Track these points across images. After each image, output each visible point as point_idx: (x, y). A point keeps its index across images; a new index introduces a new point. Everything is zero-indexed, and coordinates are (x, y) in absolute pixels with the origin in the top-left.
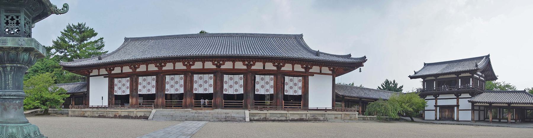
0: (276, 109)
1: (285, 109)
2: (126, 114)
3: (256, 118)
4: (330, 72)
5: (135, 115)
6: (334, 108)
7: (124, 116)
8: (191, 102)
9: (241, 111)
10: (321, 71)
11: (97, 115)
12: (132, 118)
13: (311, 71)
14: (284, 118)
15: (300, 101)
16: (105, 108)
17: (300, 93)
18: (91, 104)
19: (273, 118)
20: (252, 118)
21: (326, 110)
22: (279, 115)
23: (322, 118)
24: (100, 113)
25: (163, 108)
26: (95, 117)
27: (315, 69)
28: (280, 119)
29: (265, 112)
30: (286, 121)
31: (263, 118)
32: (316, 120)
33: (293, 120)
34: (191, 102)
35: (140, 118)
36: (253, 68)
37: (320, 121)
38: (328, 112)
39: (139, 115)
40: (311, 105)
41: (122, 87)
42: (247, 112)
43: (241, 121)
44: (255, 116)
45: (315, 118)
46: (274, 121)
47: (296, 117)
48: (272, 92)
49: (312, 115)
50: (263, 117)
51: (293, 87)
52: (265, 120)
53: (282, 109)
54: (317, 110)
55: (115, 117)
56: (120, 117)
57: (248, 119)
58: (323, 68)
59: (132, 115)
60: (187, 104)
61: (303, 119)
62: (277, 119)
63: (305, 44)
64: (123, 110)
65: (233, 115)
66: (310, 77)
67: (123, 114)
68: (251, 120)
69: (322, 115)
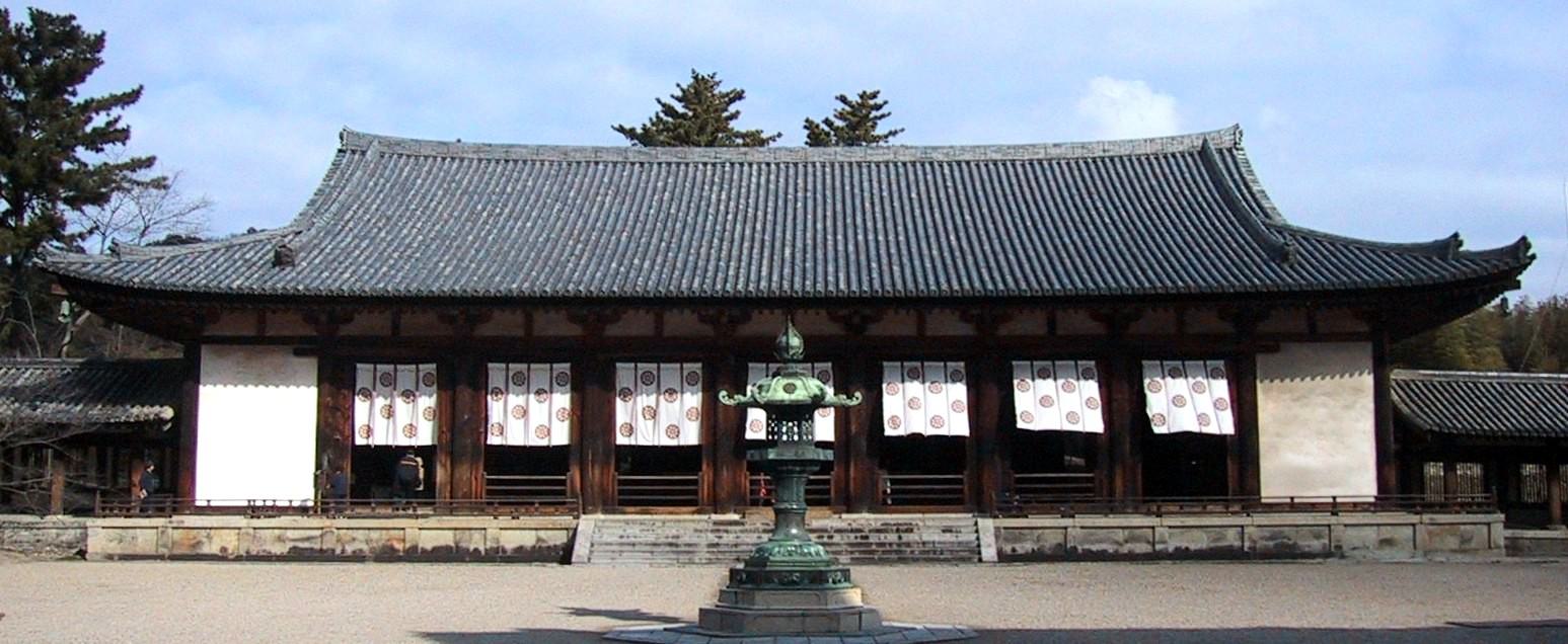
2: (446, 539)
4: (1364, 328)
6: (1383, 502)
9: (962, 520)
10: (1312, 327)
12: (476, 557)
13: (1263, 327)
14: (1142, 548)
15: (1218, 469)
18: (201, 497)
19: (1094, 548)
20: (1008, 548)
21: (1334, 507)
25: (605, 512)
26: (268, 558)
28: (1125, 549)
32: (1283, 552)
33: (1182, 555)
35: (522, 556)
36: (1003, 331)
41: (398, 418)
42: (987, 524)
43: (963, 560)
44: (1017, 540)
47: (1199, 541)
49: (1266, 532)
50: (1052, 540)
51: (1187, 403)
52: (1065, 554)
54: (1293, 506)
56: (415, 555)
57: (989, 553)
59: (476, 542)
60: (723, 495)
62: (1111, 548)
64: (433, 522)
68: (1004, 558)
69: (1316, 531)
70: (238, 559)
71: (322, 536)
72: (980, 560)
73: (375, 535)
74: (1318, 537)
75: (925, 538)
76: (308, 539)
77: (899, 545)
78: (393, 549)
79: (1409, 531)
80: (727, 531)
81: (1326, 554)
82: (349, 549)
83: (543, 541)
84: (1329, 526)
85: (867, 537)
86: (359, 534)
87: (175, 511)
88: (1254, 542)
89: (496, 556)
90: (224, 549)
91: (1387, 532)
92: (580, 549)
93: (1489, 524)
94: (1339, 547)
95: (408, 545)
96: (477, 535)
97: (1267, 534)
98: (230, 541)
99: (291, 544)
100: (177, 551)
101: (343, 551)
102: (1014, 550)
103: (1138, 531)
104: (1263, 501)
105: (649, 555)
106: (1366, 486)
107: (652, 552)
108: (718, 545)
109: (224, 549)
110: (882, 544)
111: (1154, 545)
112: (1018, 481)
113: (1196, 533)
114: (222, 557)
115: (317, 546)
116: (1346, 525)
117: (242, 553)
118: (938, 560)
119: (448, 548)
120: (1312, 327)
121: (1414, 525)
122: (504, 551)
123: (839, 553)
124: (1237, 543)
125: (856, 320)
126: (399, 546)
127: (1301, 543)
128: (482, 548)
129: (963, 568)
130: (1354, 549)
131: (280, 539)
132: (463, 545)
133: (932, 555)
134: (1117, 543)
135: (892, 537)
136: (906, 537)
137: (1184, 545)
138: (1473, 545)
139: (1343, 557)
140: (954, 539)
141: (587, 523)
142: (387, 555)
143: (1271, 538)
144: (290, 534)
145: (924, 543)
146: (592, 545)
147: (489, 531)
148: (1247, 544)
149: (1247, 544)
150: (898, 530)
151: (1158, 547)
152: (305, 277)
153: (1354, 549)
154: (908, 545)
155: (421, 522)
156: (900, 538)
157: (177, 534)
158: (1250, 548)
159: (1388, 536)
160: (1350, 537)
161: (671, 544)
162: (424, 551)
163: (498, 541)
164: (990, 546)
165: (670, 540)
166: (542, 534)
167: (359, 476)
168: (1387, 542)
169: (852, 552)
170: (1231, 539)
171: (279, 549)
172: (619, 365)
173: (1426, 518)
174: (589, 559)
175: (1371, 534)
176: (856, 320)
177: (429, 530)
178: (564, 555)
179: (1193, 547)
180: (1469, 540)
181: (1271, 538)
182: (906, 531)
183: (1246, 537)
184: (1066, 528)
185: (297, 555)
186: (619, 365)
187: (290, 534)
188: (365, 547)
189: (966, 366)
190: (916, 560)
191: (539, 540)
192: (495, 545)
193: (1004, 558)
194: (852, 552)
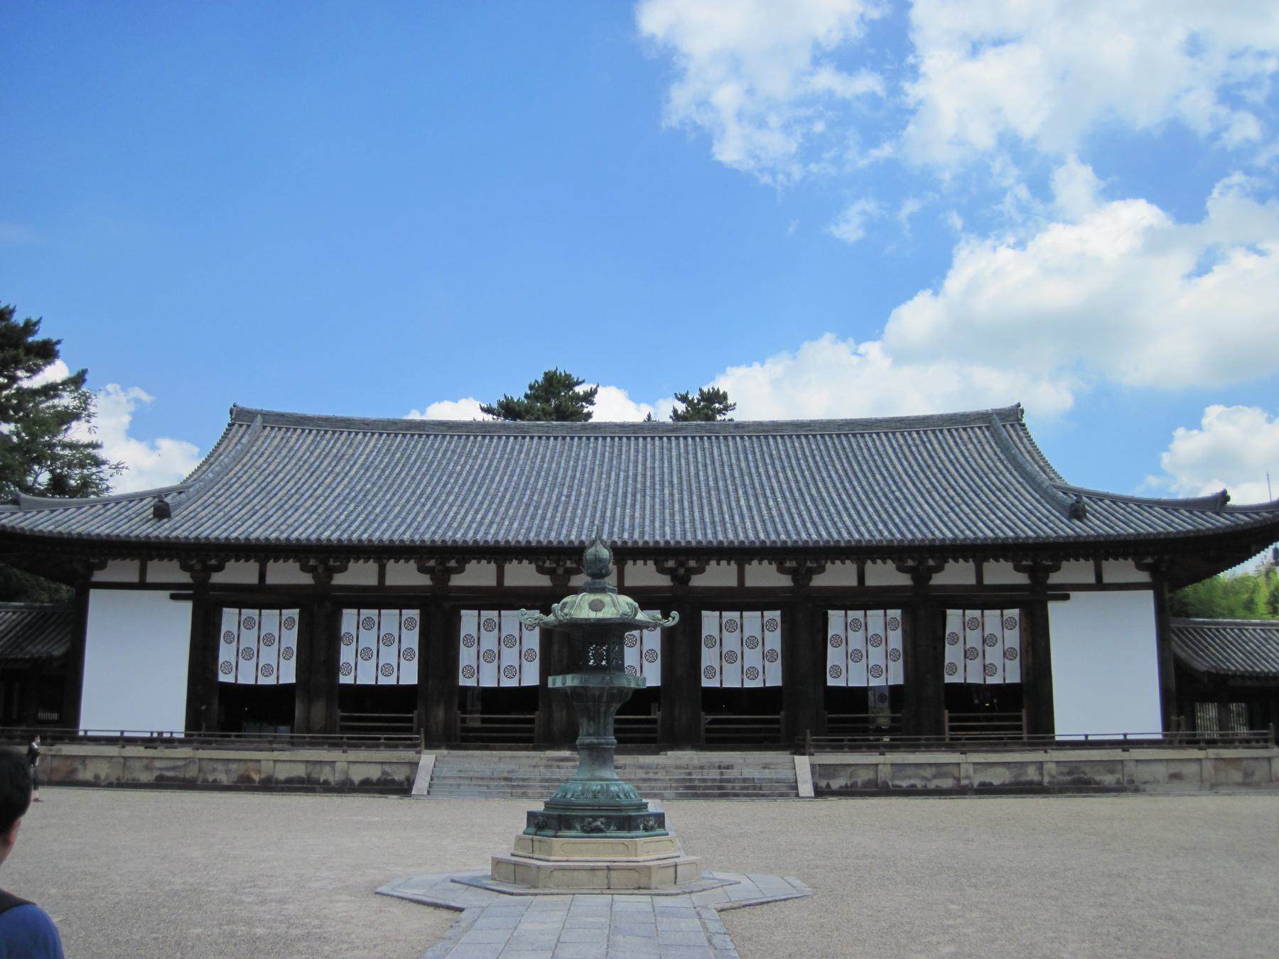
0: (914, 747)
1: (951, 747)
2: (300, 771)
3: (836, 784)
7: (290, 781)
12: (327, 788)
14: (947, 783)
17: (1011, 674)
19: (905, 784)
20: (823, 784)
21: (1125, 744)
22: (928, 773)
23: (1109, 779)
24: (144, 768)
25: (450, 747)
26: (136, 785)
28: (932, 785)
29: (874, 758)
31: (867, 784)
32: (1079, 784)
33: (986, 790)
37: (1102, 790)
38: (1137, 754)
39: (358, 774)
40: (1064, 727)
43: (781, 795)
46: (911, 792)
47: (999, 777)
48: (896, 675)
50: (863, 776)
56: (269, 785)
57: (806, 788)
59: (325, 774)
62: (920, 784)
63: (1034, 452)
64: (286, 755)
65: (747, 773)
66: (1054, 608)
67: (282, 773)
69: (1110, 766)
70: (110, 786)
71: (185, 766)
72: (797, 795)
73: (233, 766)
74: (1112, 772)
75: (746, 775)
76: (173, 768)
77: (721, 781)
78: (250, 779)
79: (1194, 768)
80: (559, 767)
82: (211, 778)
83: (388, 774)
84: (1122, 761)
85: (690, 774)
86: (220, 766)
87: (58, 739)
88: (1052, 777)
89: (346, 787)
90: (97, 777)
91: (1175, 768)
92: (421, 784)
93: (1269, 759)
94: (1132, 782)
95: (263, 776)
96: (327, 769)
97: (1065, 770)
98: (103, 770)
99: (157, 773)
100: (55, 777)
101: (205, 781)
102: (828, 786)
103: (945, 769)
104: (1057, 738)
105: (485, 789)
107: (488, 786)
108: (547, 780)
109: (97, 777)
110: (704, 780)
111: (958, 780)
112: (831, 721)
113: (1000, 770)
114: (95, 784)
115: (180, 774)
116: (1137, 761)
117: (113, 779)
118: (757, 795)
119: (300, 780)
121: (1199, 760)
122: (352, 783)
123: (665, 789)
124: (1036, 778)
125: (682, 571)
126: (256, 777)
127: (1098, 778)
128: (331, 779)
129: (781, 804)
130: (1145, 783)
131: (148, 768)
132: (315, 776)
133: (752, 790)
134: (924, 778)
135: (714, 774)
136: (729, 774)
137: (988, 780)
138: (1256, 778)
139: (1137, 790)
140: (773, 776)
141: (427, 759)
142: (244, 784)
143: (1069, 773)
144: (158, 764)
145: (744, 780)
146: (432, 779)
147: (338, 765)
148: (1046, 780)
149: (1046, 780)
150: (720, 767)
151: (964, 782)
152: (178, 528)
153: (1145, 783)
154: (729, 781)
155: (276, 755)
156: (722, 774)
157: (56, 763)
158: (1050, 783)
159: (1176, 770)
160: (1142, 773)
161: (506, 779)
162: (278, 781)
163: (347, 773)
164: (806, 782)
165: (506, 775)
166: (387, 768)
167: (222, 710)
168: (1176, 776)
169: (676, 788)
170: (1032, 774)
171: (146, 777)
172: (463, 612)
173: (1212, 753)
174: (429, 793)
175: (1162, 771)
176: (682, 571)
177: (285, 761)
178: (403, 789)
179: (996, 782)
180: (1252, 774)
181: (1069, 773)
182: (727, 767)
183: (1045, 773)
184: (877, 765)
185: (162, 783)
186: (463, 612)
187: (158, 764)
188: (224, 779)
189: (782, 616)
190: (737, 795)
191: (384, 773)
192: (343, 778)
193: (820, 793)
194: (676, 788)
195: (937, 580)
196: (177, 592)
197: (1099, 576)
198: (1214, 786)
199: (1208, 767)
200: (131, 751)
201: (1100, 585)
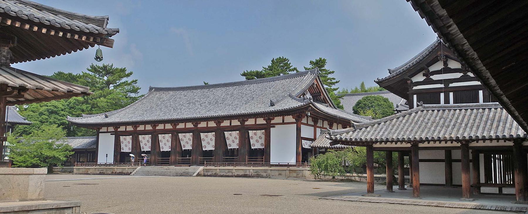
5: (126, 172)
8: (176, 159)
11: (98, 172)
14: (230, 174)
16: (110, 165)
19: (222, 174)
23: (264, 174)
27: (278, 119)
30: (232, 176)
34: (176, 159)
37: (262, 177)
44: (209, 172)
45: (258, 174)
53: (245, 165)
55: (112, 174)
58: (286, 117)
61: (247, 175)
64: (118, 167)
81: (267, 177)
106: (293, 161)
120: (283, 121)
138: (299, 176)
160: (273, 173)
168: (280, 174)
170: (248, 173)
195: (246, 123)
196: (112, 133)
197: (283, 121)
198: (288, 177)
199: (288, 172)
200: (102, 167)
201: (283, 123)
